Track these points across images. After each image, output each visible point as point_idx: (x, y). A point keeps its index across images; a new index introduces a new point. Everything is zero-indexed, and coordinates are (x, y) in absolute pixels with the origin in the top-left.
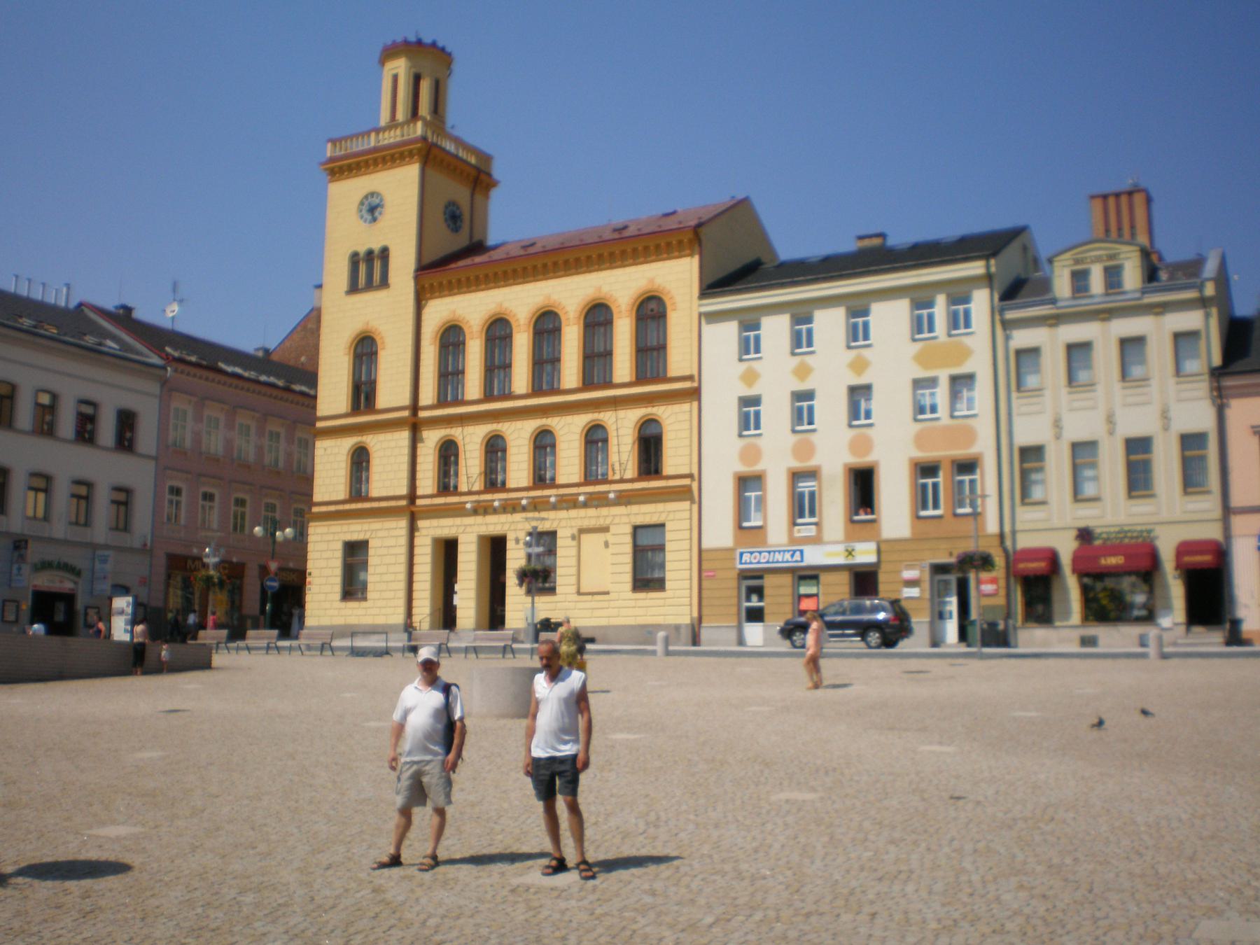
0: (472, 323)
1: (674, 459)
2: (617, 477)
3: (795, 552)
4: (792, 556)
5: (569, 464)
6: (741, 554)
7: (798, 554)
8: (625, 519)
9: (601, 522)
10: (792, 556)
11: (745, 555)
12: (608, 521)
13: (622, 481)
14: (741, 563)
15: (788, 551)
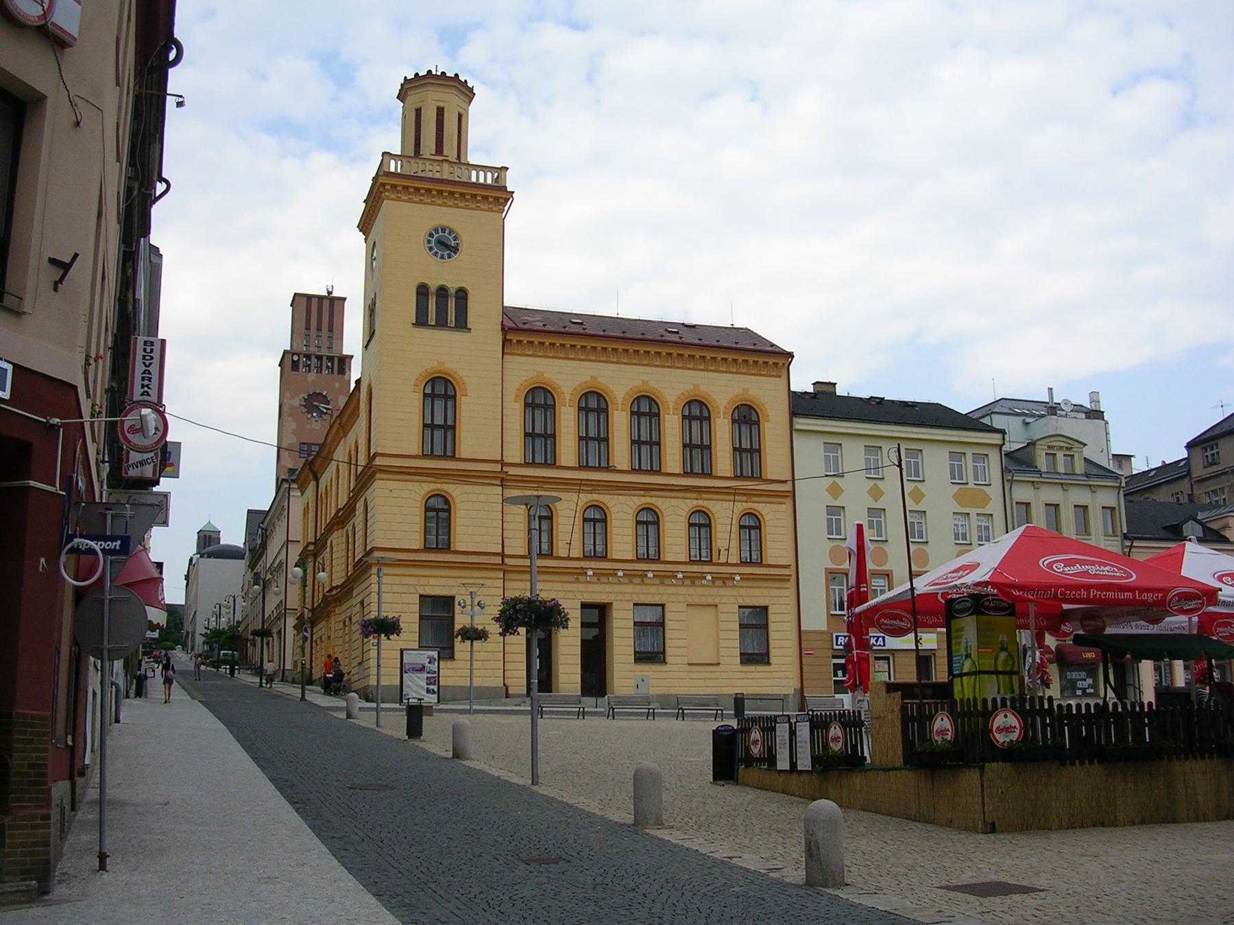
0: (565, 390)
1: (776, 550)
2: (723, 560)
3: (878, 637)
4: (877, 641)
5: (676, 542)
6: (837, 637)
7: (881, 639)
8: (732, 600)
9: (710, 601)
10: (877, 641)
11: (840, 638)
12: (717, 600)
13: (727, 564)
14: (837, 645)
15: (874, 637)
